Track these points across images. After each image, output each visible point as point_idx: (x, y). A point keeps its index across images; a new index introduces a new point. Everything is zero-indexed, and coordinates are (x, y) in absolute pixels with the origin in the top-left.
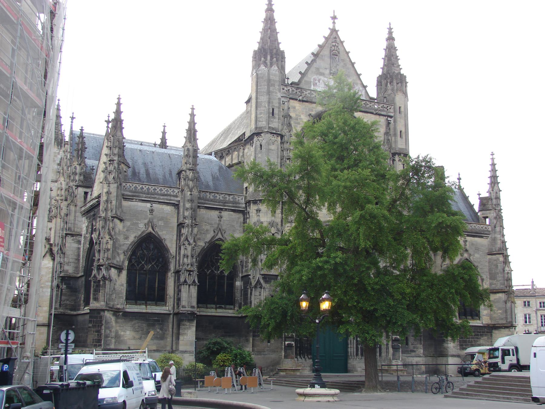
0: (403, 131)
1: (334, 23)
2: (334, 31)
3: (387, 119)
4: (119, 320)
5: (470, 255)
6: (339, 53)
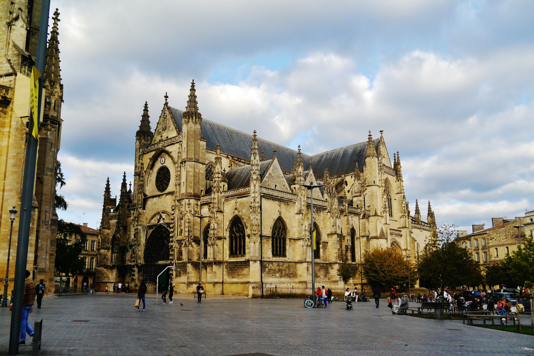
0: (186, 147)
1: (166, 100)
2: (166, 104)
3: (179, 144)
4: (109, 270)
5: (239, 212)
6: (166, 116)
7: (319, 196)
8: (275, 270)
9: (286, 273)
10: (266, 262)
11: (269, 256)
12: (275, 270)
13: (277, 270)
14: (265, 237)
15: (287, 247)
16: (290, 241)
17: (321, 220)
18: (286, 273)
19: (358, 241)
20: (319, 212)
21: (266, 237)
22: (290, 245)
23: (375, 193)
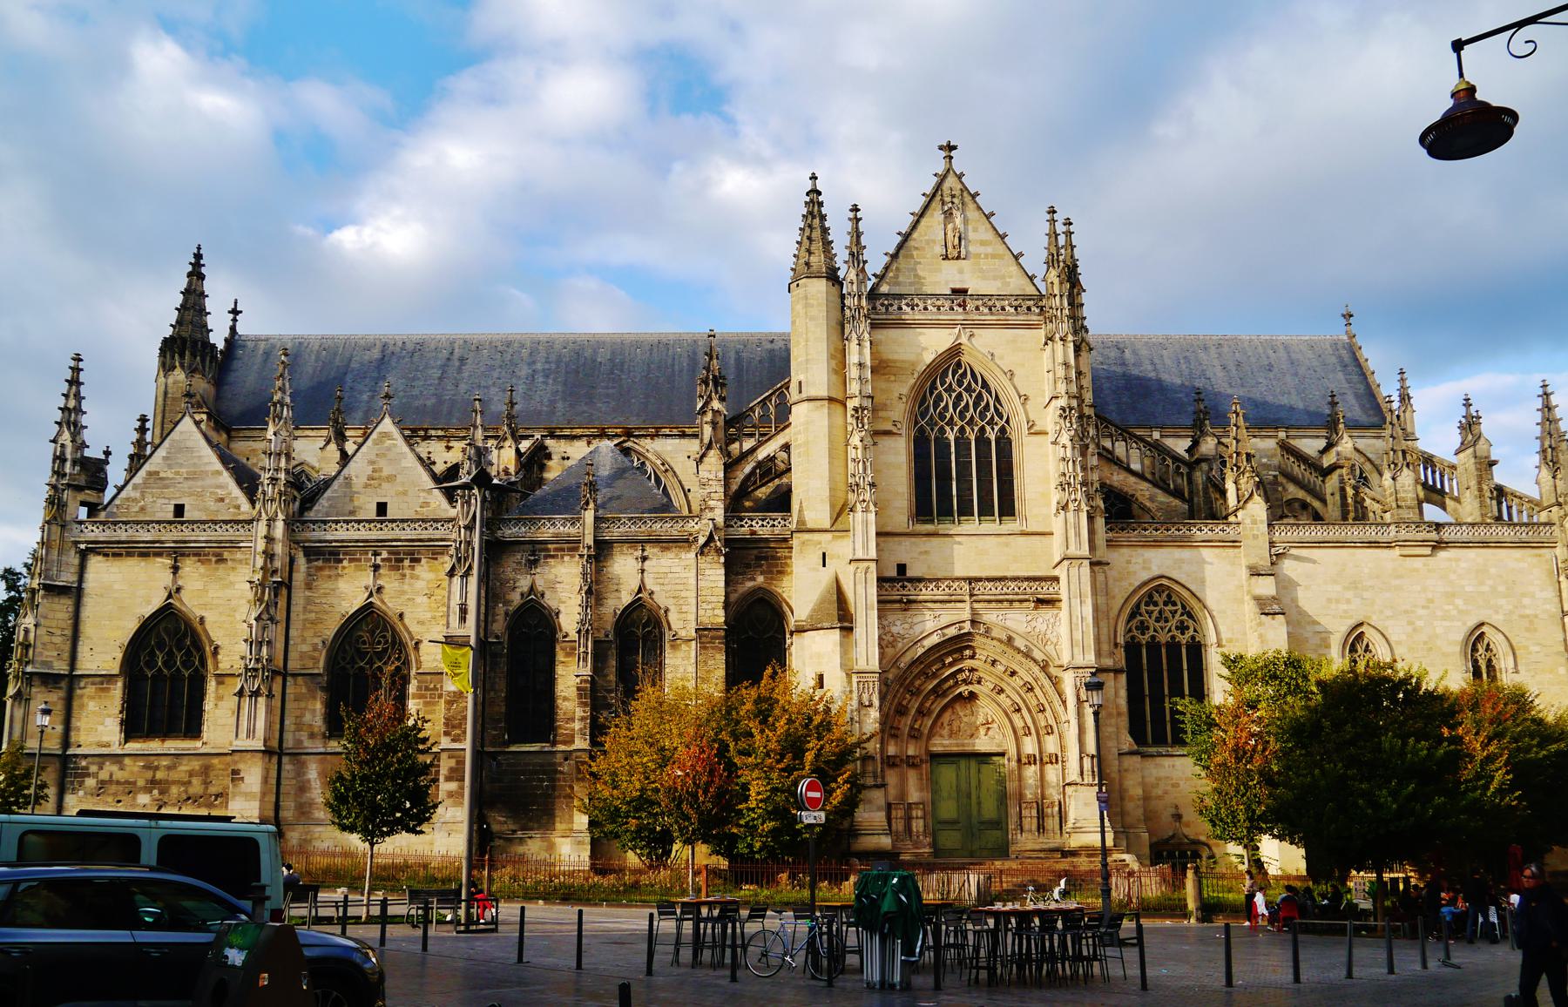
7: (426, 504)
8: (134, 783)
9: (186, 792)
10: (90, 759)
11: (105, 739)
12: (134, 783)
13: (141, 783)
14: (91, 680)
15: (208, 705)
16: (219, 683)
17: (417, 593)
18: (186, 792)
19: (680, 654)
20: (407, 563)
21: (98, 679)
22: (219, 698)
23: (799, 432)
